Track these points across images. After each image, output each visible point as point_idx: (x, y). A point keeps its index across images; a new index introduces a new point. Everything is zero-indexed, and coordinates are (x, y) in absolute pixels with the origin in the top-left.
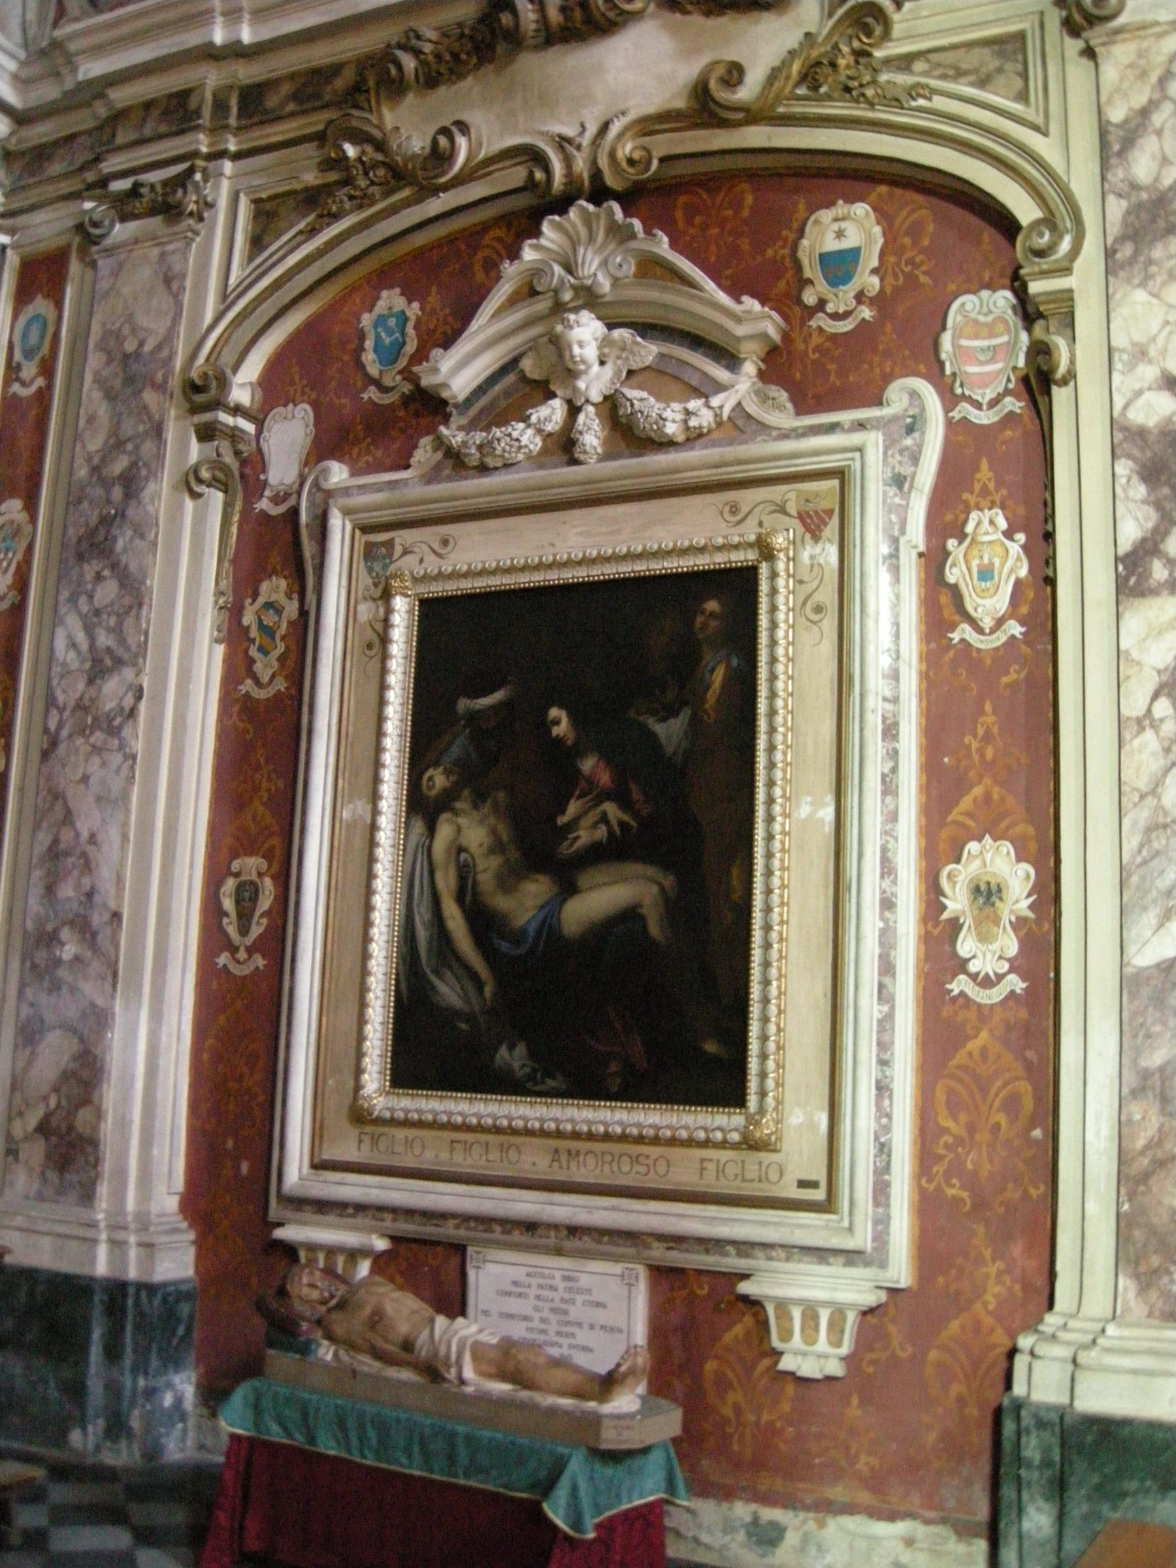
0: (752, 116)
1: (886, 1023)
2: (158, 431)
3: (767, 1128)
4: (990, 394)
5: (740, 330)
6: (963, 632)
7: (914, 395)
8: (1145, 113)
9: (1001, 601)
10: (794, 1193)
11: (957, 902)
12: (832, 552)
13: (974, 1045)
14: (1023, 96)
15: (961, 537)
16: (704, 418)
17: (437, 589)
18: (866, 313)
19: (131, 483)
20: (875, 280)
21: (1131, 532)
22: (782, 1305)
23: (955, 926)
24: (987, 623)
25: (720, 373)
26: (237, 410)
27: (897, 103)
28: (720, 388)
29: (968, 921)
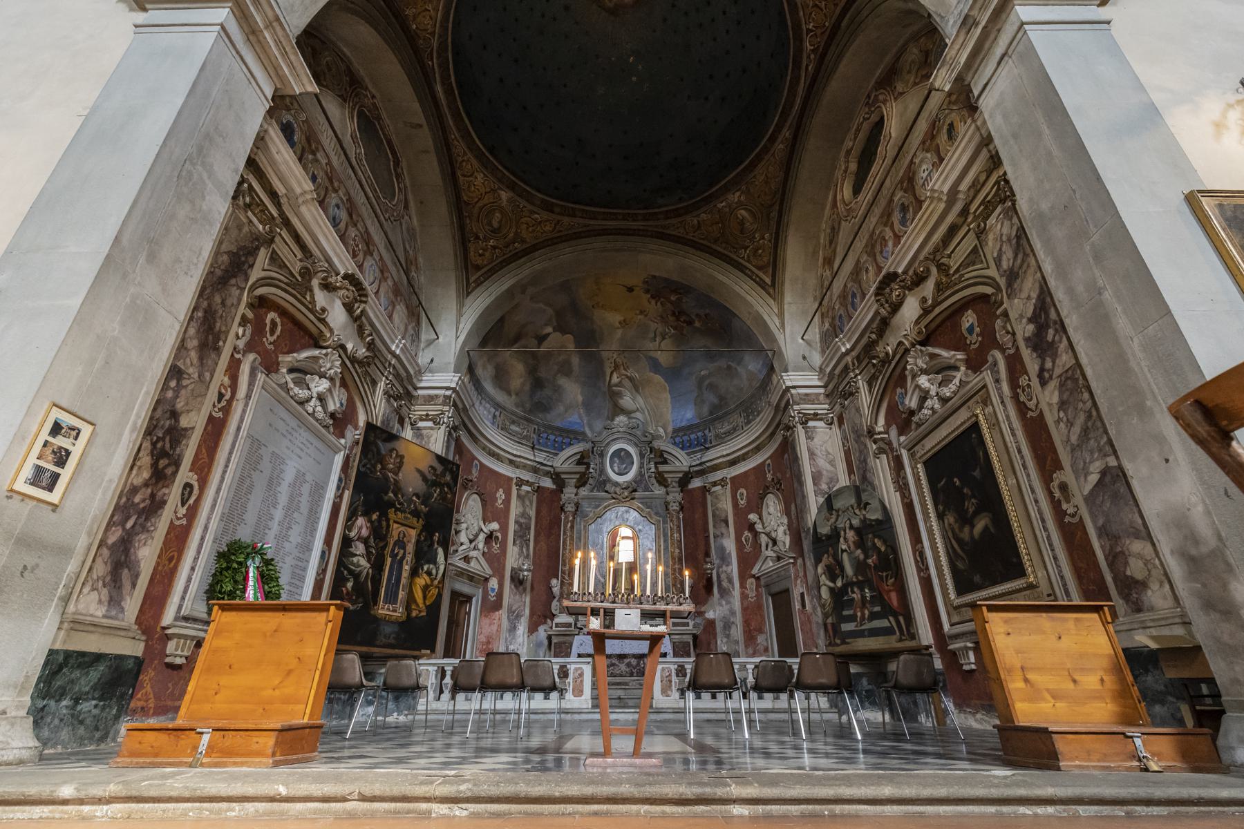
0: (934, 306)
1: (1049, 537)
2: (865, 445)
5: (953, 361)
7: (993, 356)
8: (1000, 249)
11: (1057, 494)
13: (1078, 537)
15: (1019, 387)
17: (925, 458)
18: (980, 339)
19: (865, 461)
23: (1059, 501)
24: (1034, 408)
25: (954, 374)
26: (880, 433)
27: (960, 282)
29: (1062, 499)
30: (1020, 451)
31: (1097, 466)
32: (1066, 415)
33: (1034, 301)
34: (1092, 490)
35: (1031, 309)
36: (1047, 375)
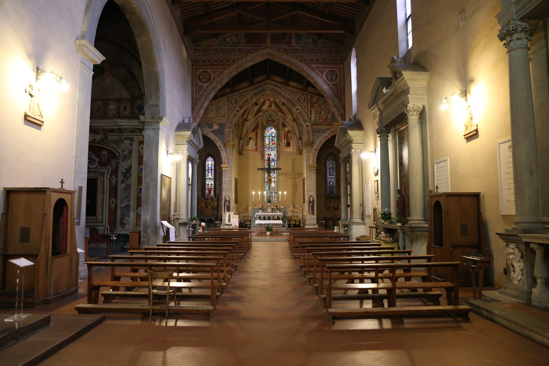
1: (106, 211)
3: (98, 218)
4: (114, 167)
6: (112, 184)
7: (109, 167)
8: (125, 149)
9: (114, 182)
10: (99, 222)
11: (111, 202)
12: (102, 178)
14: (117, 145)
16: (93, 167)
20: (107, 157)
21: (122, 179)
22: (99, 229)
23: (111, 204)
28: (94, 164)
30: (106, 191)
31: (126, 203)
32: (124, 191)
33: (128, 166)
34: (123, 207)
35: (127, 167)
36: (124, 182)
